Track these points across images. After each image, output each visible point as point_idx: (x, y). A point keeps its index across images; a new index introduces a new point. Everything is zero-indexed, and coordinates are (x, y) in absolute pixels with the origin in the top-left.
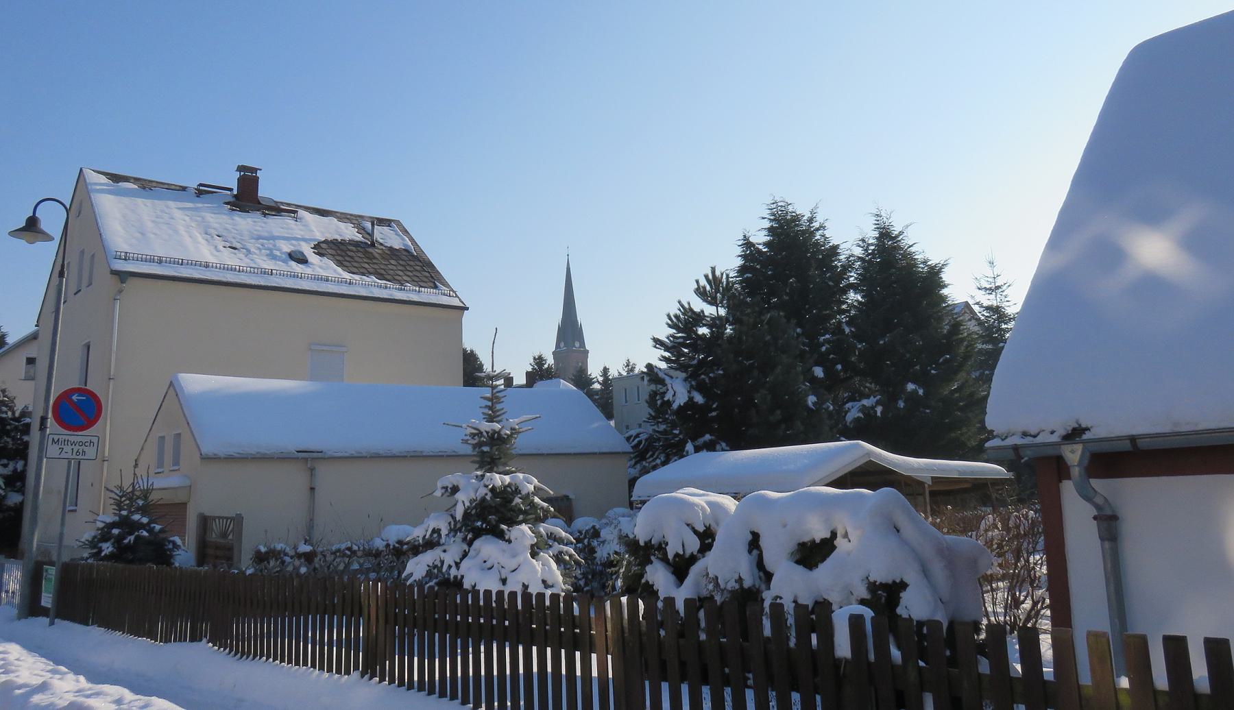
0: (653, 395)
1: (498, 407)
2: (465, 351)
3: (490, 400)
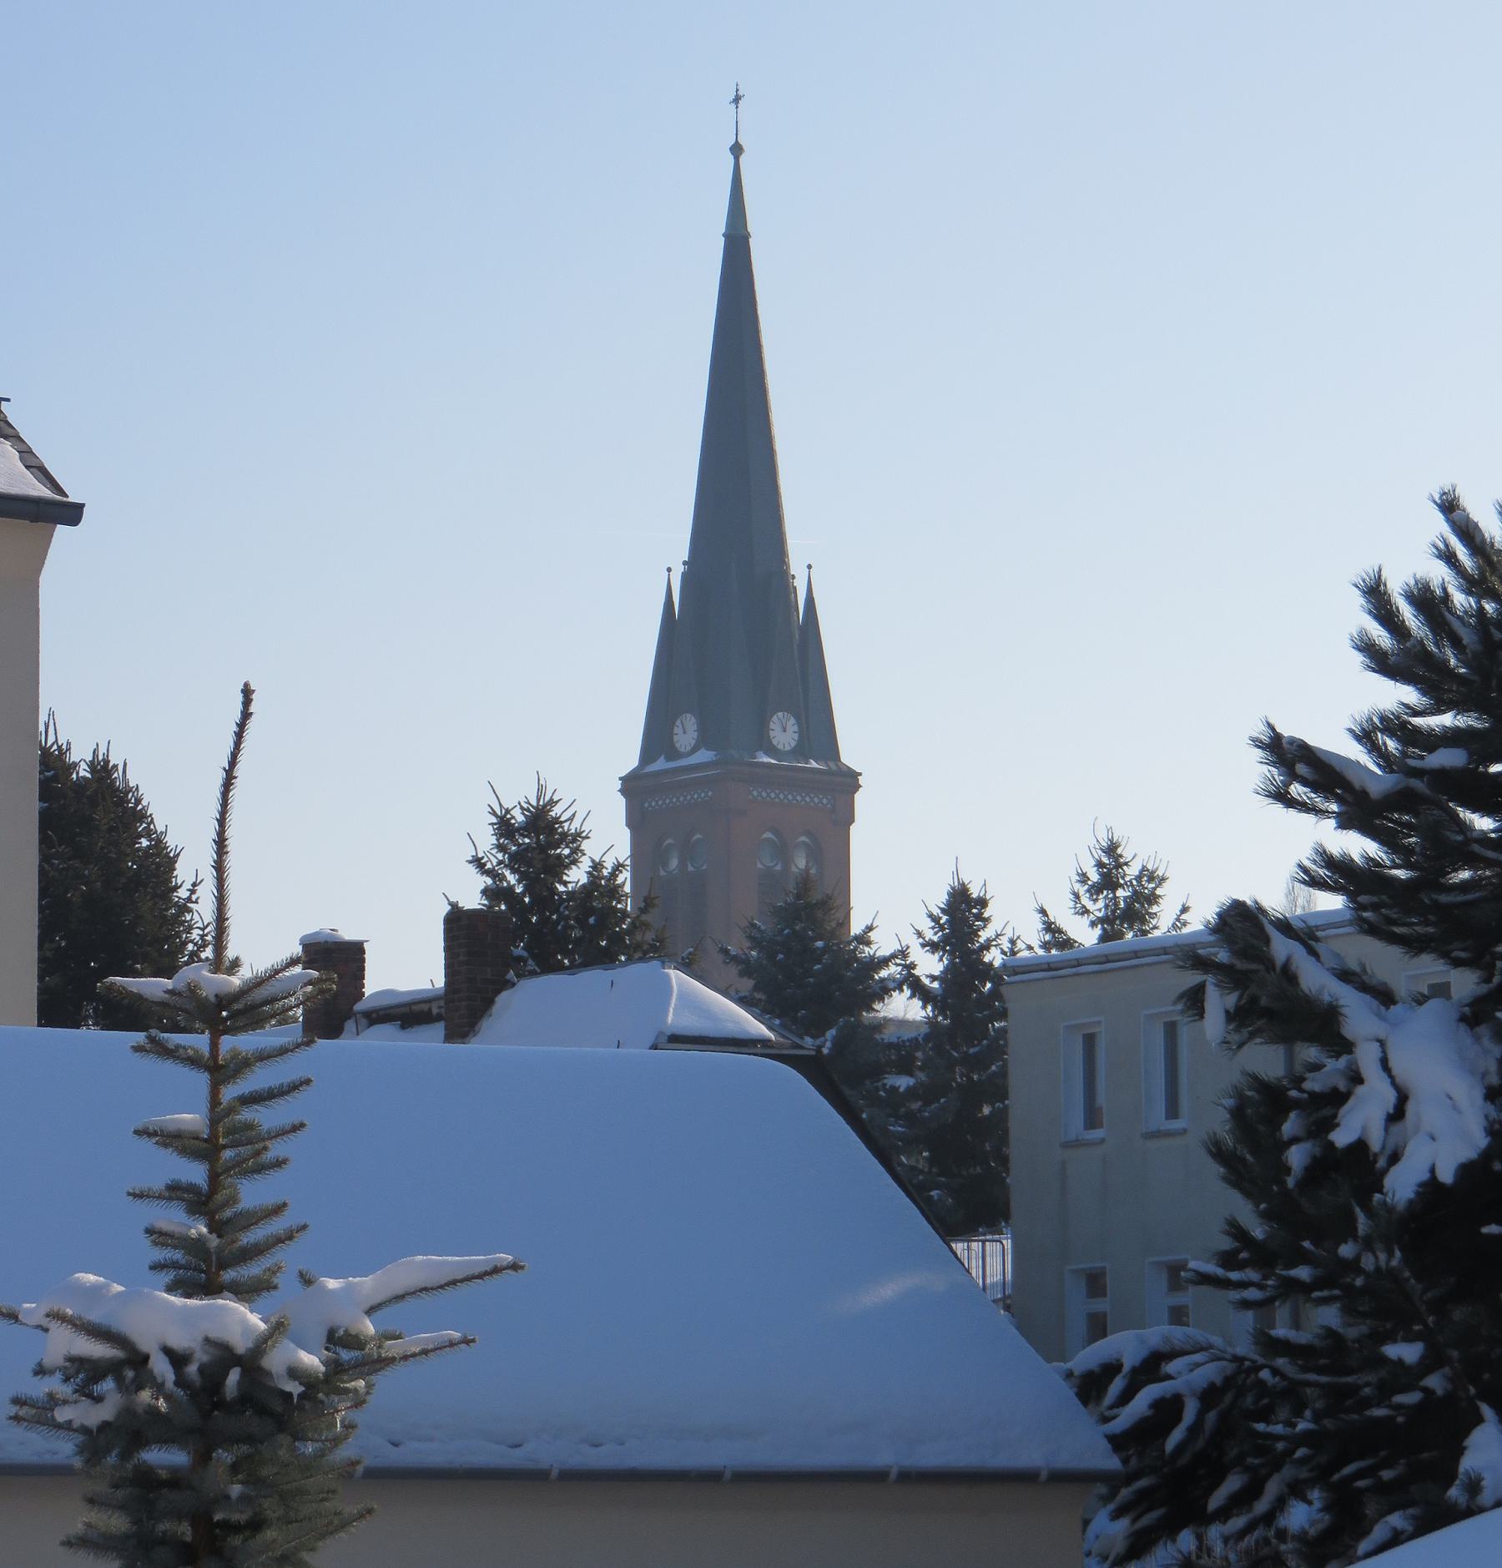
0: (1261, 1110)
1: (251, 1193)
2: (53, 763)
3: (201, 1147)
